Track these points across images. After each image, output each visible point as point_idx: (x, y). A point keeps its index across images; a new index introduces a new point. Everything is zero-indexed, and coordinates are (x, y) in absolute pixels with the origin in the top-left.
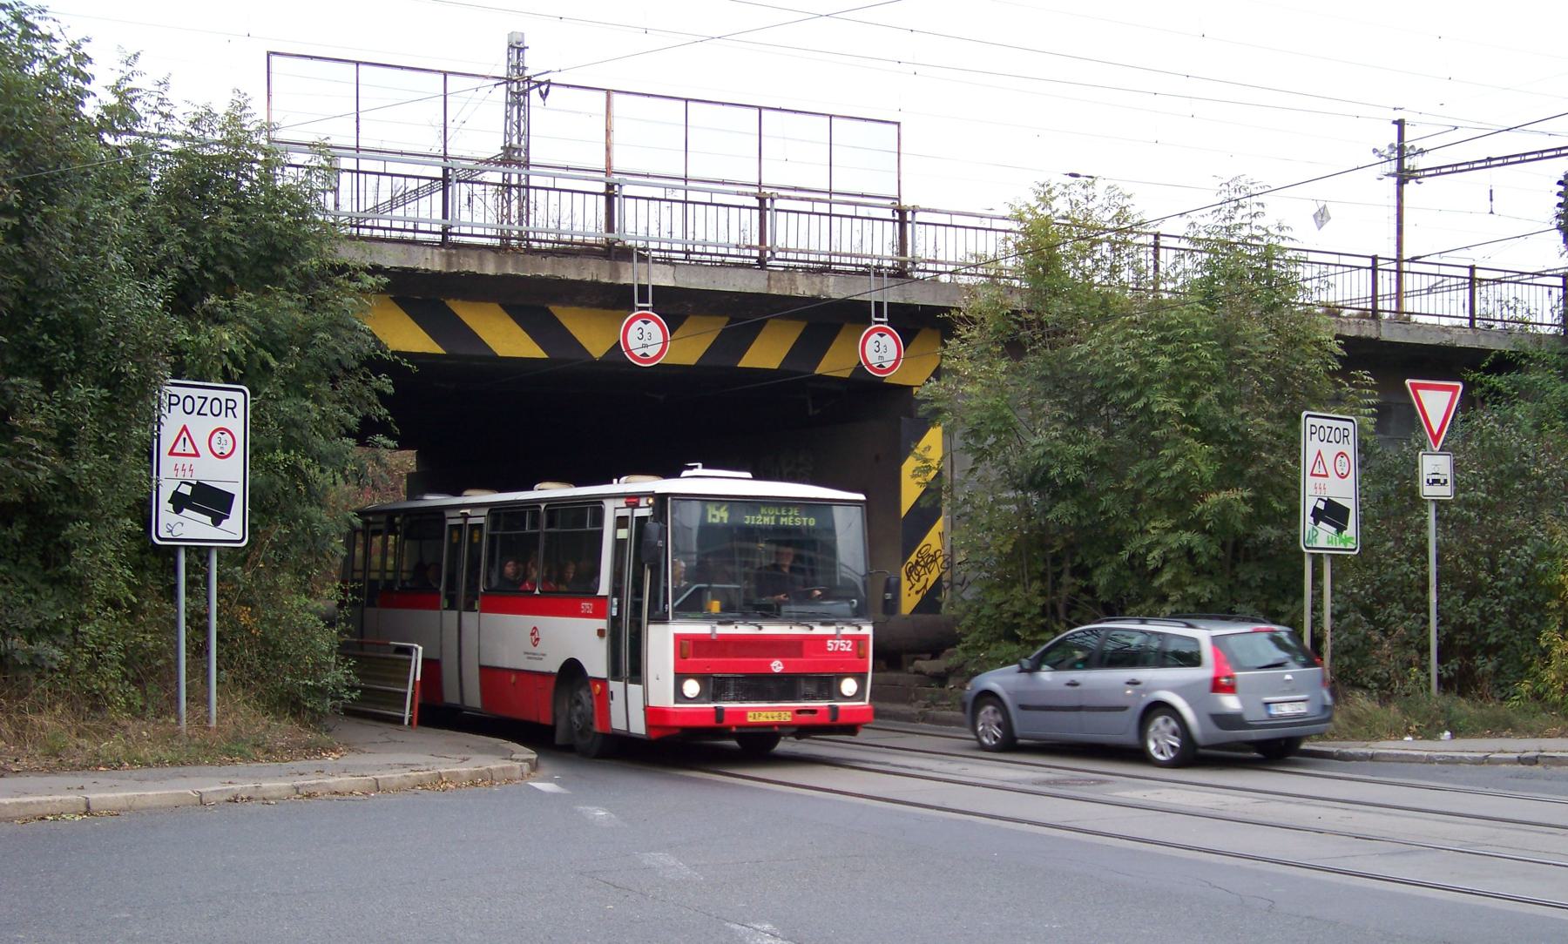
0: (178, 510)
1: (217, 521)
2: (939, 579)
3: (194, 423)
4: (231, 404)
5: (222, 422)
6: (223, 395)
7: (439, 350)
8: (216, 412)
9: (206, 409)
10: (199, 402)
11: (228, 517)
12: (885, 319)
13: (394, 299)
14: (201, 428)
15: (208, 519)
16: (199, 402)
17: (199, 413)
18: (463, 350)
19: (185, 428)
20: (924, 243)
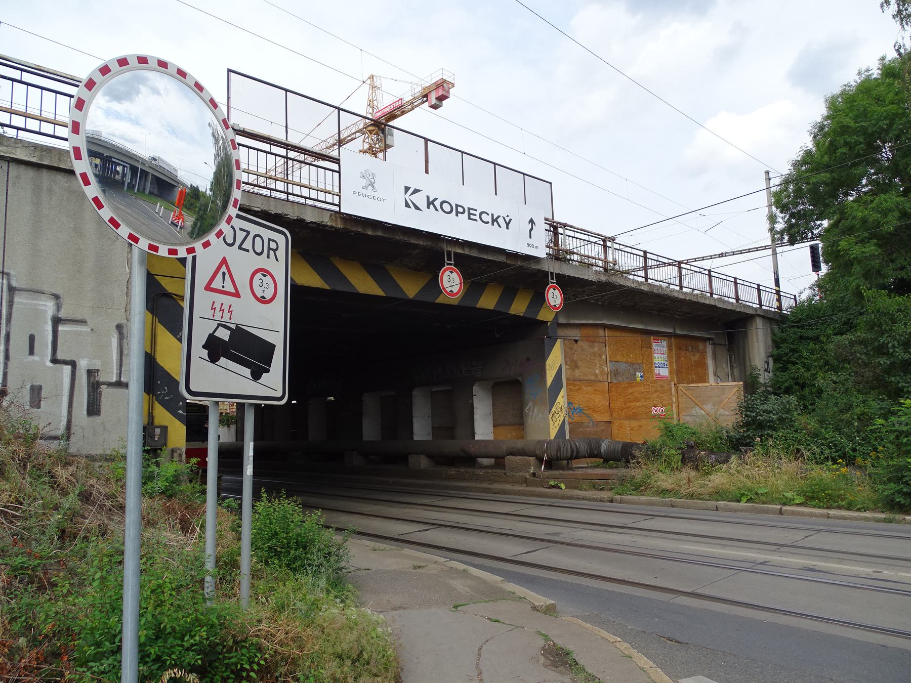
0: (213, 358)
1: (256, 376)
2: (564, 419)
3: (232, 255)
4: (273, 245)
8: (259, 250)
9: (248, 245)
10: (241, 235)
11: (268, 371)
13: (298, 252)
15: (247, 372)
17: (240, 248)
18: (340, 288)
19: (224, 261)
20: (568, 242)
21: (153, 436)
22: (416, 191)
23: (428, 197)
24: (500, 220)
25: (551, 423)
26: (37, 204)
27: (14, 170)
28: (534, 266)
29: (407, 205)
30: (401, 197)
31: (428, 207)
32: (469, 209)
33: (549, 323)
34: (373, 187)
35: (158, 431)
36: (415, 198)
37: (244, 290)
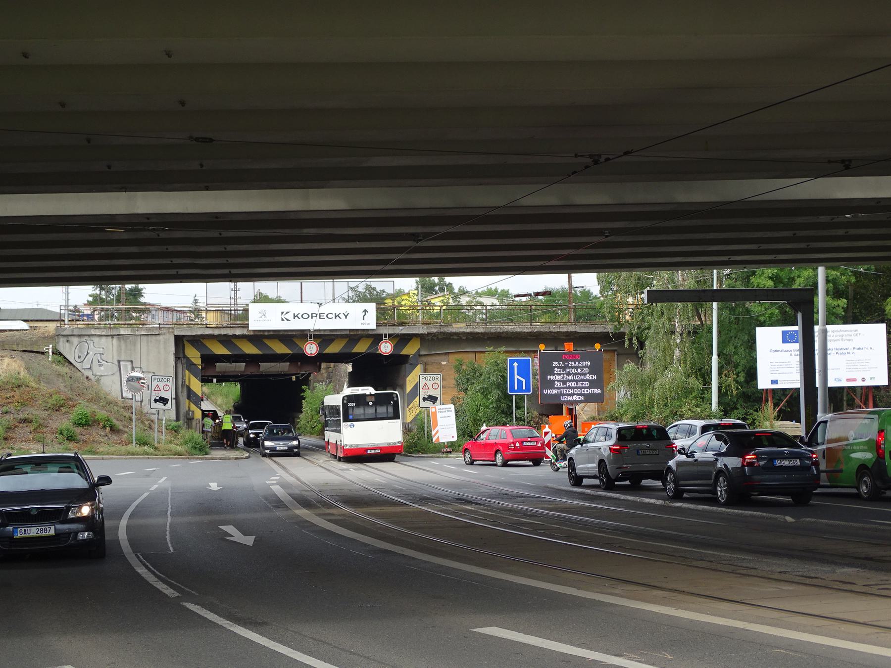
0: (155, 402)
1: (165, 405)
5: (166, 383)
7: (260, 353)
9: (163, 381)
12: (387, 338)
14: (161, 385)
15: (163, 404)
21: (189, 414)
22: (287, 313)
23: (294, 314)
24: (342, 316)
25: (408, 413)
26: (148, 346)
27: (142, 337)
28: (374, 333)
29: (283, 320)
30: (280, 316)
31: (294, 318)
32: (320, 314)
33: (411, 356)
34: (265, 316)
35: (191, 412)
36: (287, 316)
37: (162, 390)
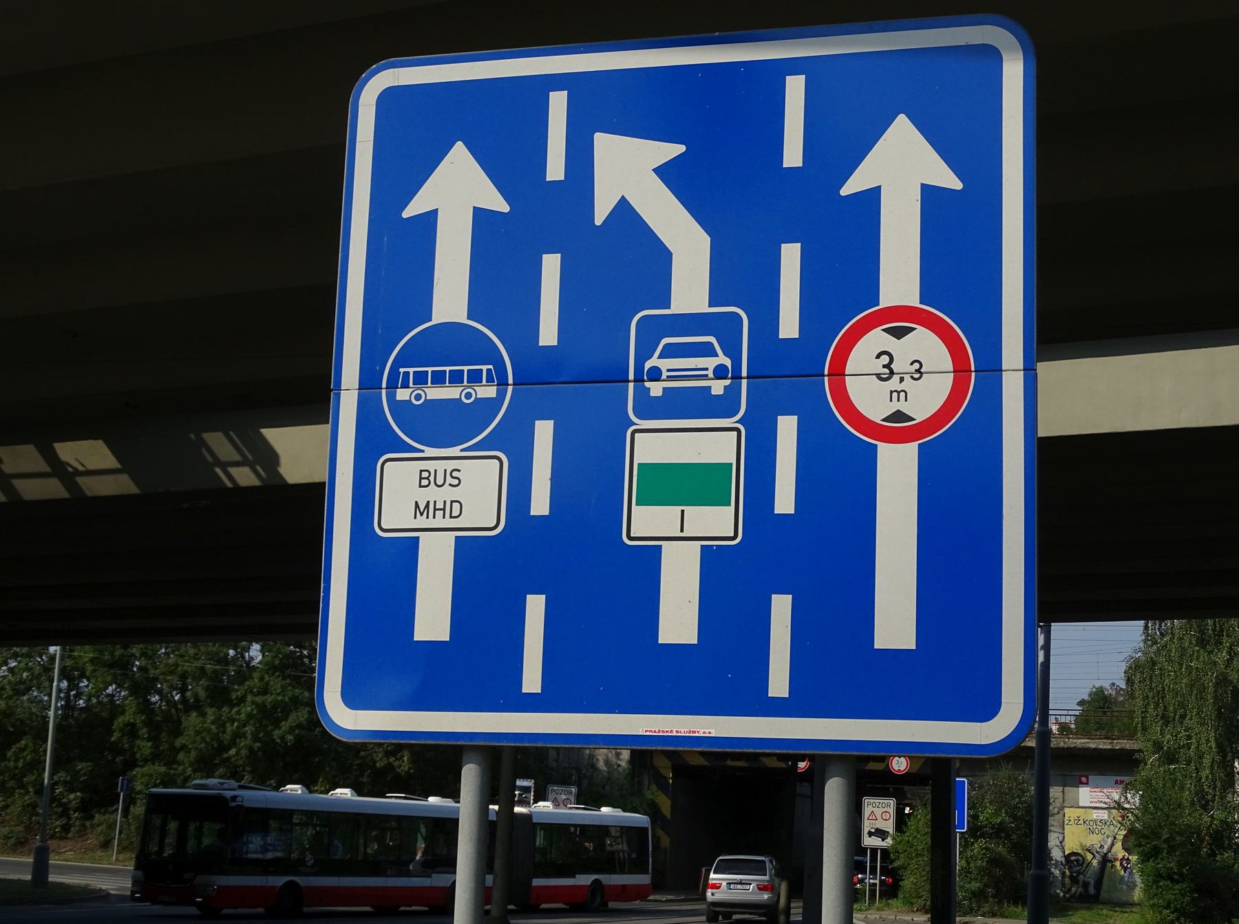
0: (870, 836)
3: (875, 810)
5: (885, 809)
6: (886, 802)
10: (880, 806)
14: (878, 812)
16: (880, 806)
37: (879, 817)
